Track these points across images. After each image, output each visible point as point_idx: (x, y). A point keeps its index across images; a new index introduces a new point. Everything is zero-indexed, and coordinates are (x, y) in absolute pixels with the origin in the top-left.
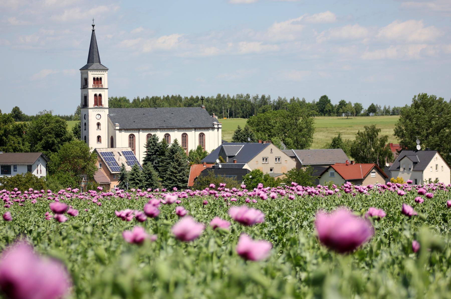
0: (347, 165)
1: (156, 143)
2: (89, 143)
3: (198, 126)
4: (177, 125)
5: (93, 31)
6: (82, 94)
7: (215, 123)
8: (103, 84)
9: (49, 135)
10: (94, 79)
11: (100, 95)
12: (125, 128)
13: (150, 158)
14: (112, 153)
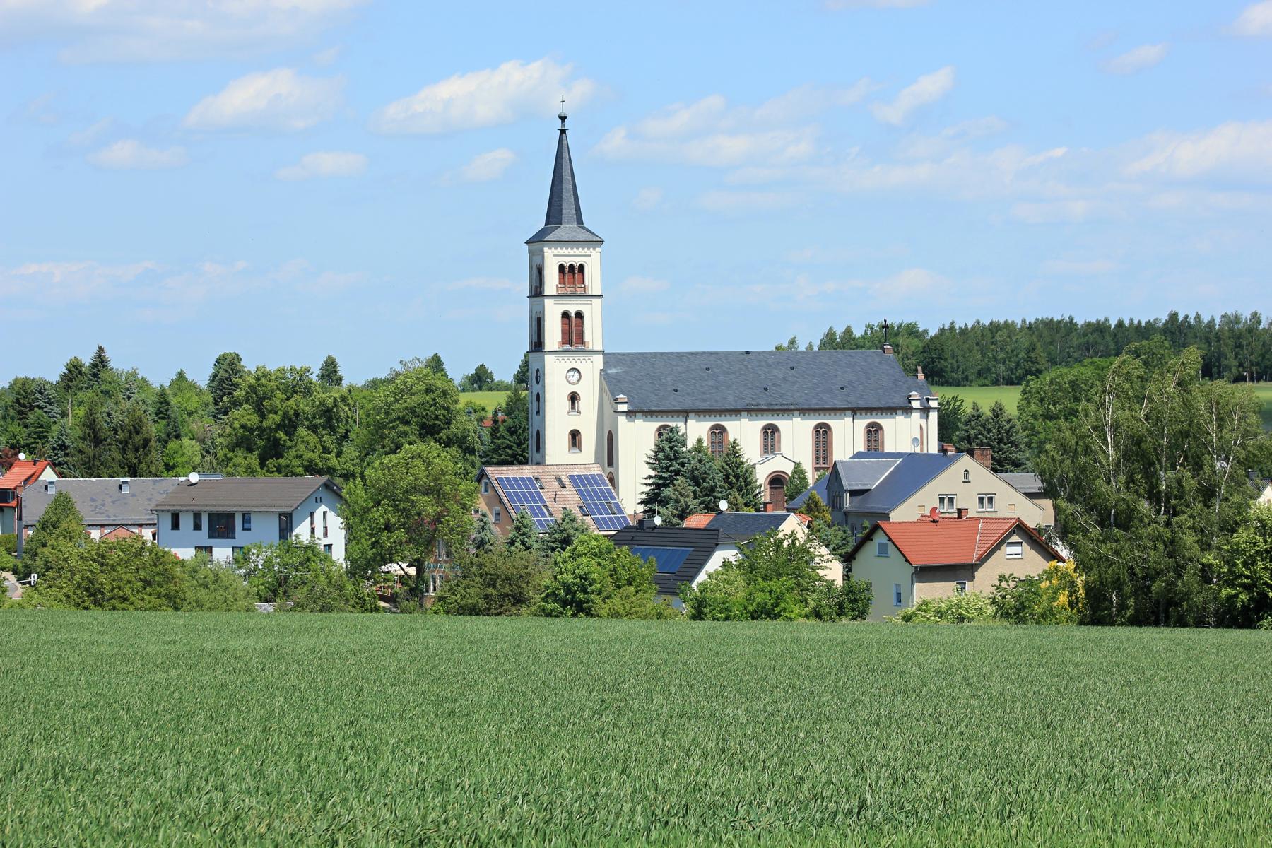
0: (934, 521)
1: (676, 451)
2: (547, 452)
3: (862, 404)
4: (800, 399)
5: (563, 132)
6: (531, 311)
7: (914, 394)
8: (586, 283)
9: (402, 428)
10: (562, 268)
11: (579, 315)
12: (645, 409)
13: (658, 495)
14: (537, 479)
